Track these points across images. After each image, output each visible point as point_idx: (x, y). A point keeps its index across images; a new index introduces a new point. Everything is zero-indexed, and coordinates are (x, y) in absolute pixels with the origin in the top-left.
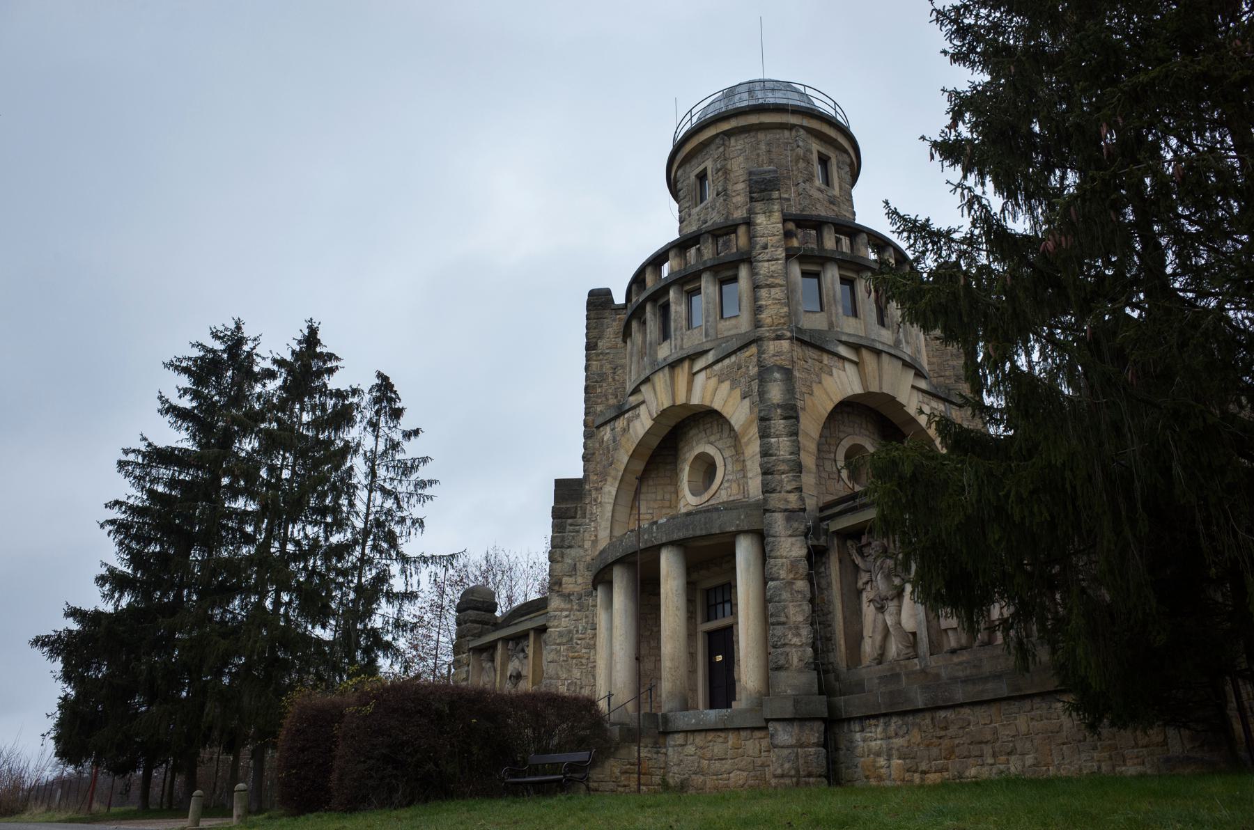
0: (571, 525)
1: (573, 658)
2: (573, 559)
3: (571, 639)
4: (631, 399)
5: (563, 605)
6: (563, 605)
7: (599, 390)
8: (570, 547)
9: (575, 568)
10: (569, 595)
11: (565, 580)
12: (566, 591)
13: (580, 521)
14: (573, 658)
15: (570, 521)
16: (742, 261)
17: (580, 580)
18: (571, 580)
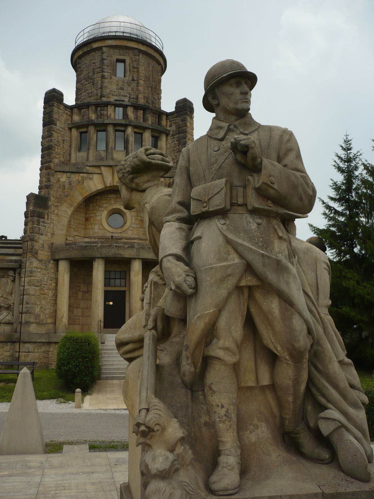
0: (43, 222)
1: (43, 294)
2: (43, 241)
3: (41, 285)
4: (87, 167)
5: (40, 266)
6: (40, 266)
7: (57, 150)
8: (42, 234)
9: (43, 245)
10: (42, 261)
11: (39, 252)
12: (39, 258)
13: (46, 221)
14: (43, 294)
15: (42, 220)
16: (165, 133)
17: (46, 254)
18: (42, 252)
